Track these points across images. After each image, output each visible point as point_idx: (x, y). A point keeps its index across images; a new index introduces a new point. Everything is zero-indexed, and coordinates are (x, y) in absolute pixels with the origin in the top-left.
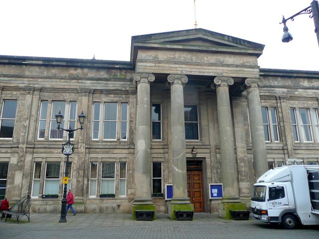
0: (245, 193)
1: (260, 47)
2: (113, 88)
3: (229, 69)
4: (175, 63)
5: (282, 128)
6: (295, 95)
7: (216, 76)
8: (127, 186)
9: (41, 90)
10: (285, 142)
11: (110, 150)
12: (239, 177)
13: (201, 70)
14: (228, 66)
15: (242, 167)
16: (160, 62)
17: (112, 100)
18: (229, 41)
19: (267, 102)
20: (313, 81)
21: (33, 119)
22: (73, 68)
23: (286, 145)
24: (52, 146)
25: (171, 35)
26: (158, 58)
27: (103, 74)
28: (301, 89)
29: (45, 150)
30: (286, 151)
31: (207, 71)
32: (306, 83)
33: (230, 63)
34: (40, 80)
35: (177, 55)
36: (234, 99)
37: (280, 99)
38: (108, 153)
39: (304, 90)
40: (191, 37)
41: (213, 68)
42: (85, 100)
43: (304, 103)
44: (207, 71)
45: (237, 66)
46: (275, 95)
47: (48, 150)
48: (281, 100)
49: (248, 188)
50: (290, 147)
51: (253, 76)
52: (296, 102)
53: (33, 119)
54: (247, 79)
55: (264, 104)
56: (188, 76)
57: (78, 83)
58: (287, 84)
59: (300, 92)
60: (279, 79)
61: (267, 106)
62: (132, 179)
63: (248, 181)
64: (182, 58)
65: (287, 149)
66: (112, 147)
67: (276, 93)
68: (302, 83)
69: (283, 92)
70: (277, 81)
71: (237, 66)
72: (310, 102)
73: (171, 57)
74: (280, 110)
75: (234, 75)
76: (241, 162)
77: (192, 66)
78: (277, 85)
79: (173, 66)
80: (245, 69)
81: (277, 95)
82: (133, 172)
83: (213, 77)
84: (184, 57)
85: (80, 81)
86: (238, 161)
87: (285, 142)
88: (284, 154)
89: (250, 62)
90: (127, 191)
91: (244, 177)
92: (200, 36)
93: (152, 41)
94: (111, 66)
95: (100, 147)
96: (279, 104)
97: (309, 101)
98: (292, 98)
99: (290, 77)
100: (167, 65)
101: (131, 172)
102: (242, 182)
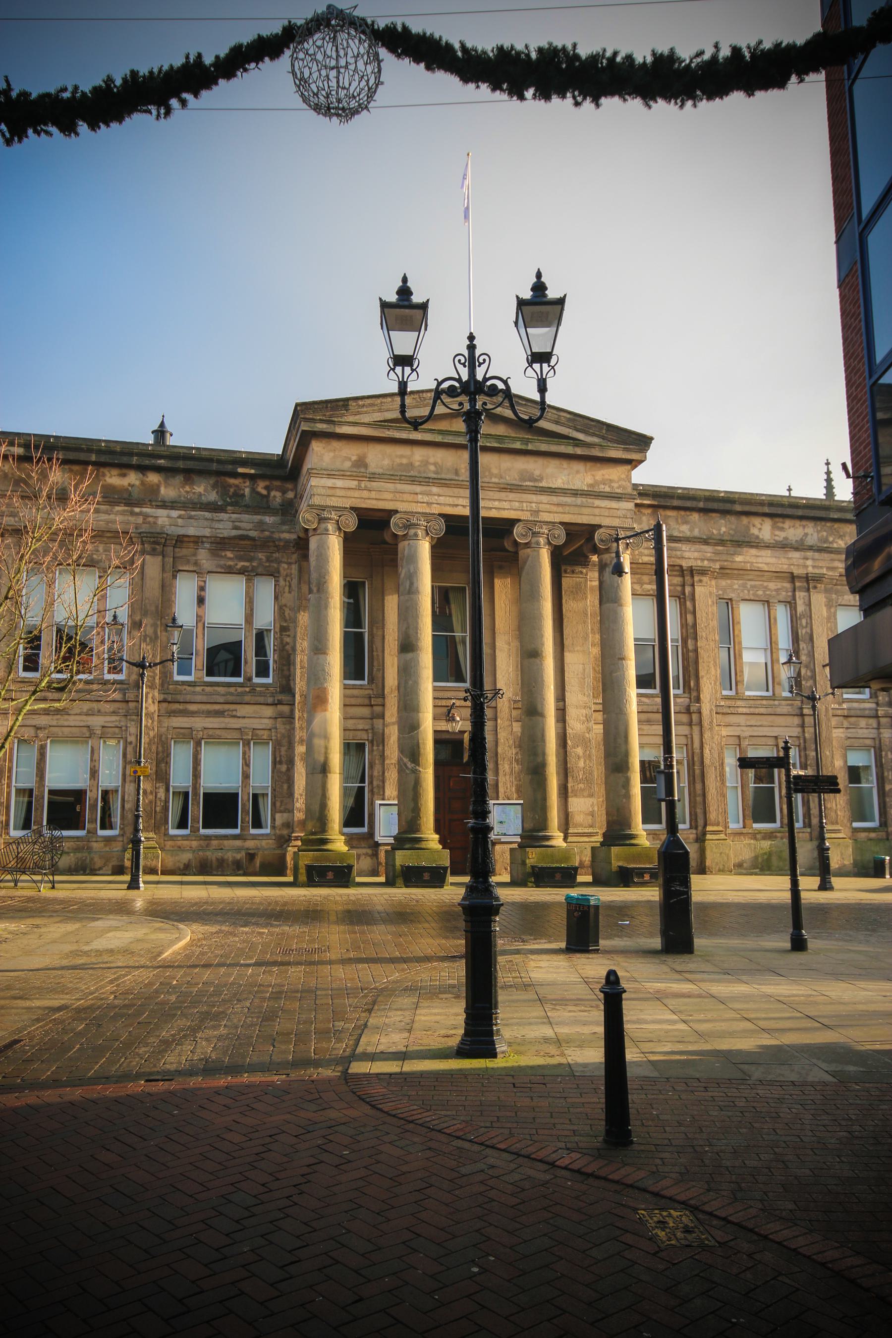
0: (581, 825)
1: (642, 442)
2: (235, 533)
3: (555, 499)
4: (413, 480)
5: (691, 654)
6: (735, 566)
7: (519, 520)
8: (274, 804)
10: (694, 694)
11: (227, 707)
12: (569, 785)
16: (373, 477)
17: (230, 566)
22: (115, 472)
23: (698, 700)
26: (366, 466)
27: (202, 489)
30: (695, 717)
31: (496, 504)
35: (418, 455)
36: (566, 572)
37: (692, 576)
38: (219, 714)
41: (512, 496)
42: (153, 565)
44: (496, 504)
48: (696, 578)
49: (592, 814)
50: (706, 707)
52: (737, 584)
54: (601, 530)
56: (447, 517)
57: (132, 514)
58: (715, 532)
59: (746, 557)
60: (695, 516)
62: (285, 786)
63: (591, 796)
65: (700, 713)
66: (231, 698)
68: (755, 531)
70: (686, 522)
71: (575, 493)
72: (772, 585)
73: (401, 464)
74: (689, 604)
75: (567, 519)
77: (456, 490)
78: (688, 534)
80: (597, 502)
81: (685, 564)
82: (288, 770)
84: (435, 464)
85: (137, 510)
86: (569, 742)
87: (694, 694)
88: (690, 724)
89: (611, 481)
90: (273, 819)
91: (581, 786)
94: (230, 467)
95: (199, 698)
96: (688, 589)
98: (724, 572)
99: (725, 513)
100: (390, 486)
101: (284, 768)
102: (576, 796)
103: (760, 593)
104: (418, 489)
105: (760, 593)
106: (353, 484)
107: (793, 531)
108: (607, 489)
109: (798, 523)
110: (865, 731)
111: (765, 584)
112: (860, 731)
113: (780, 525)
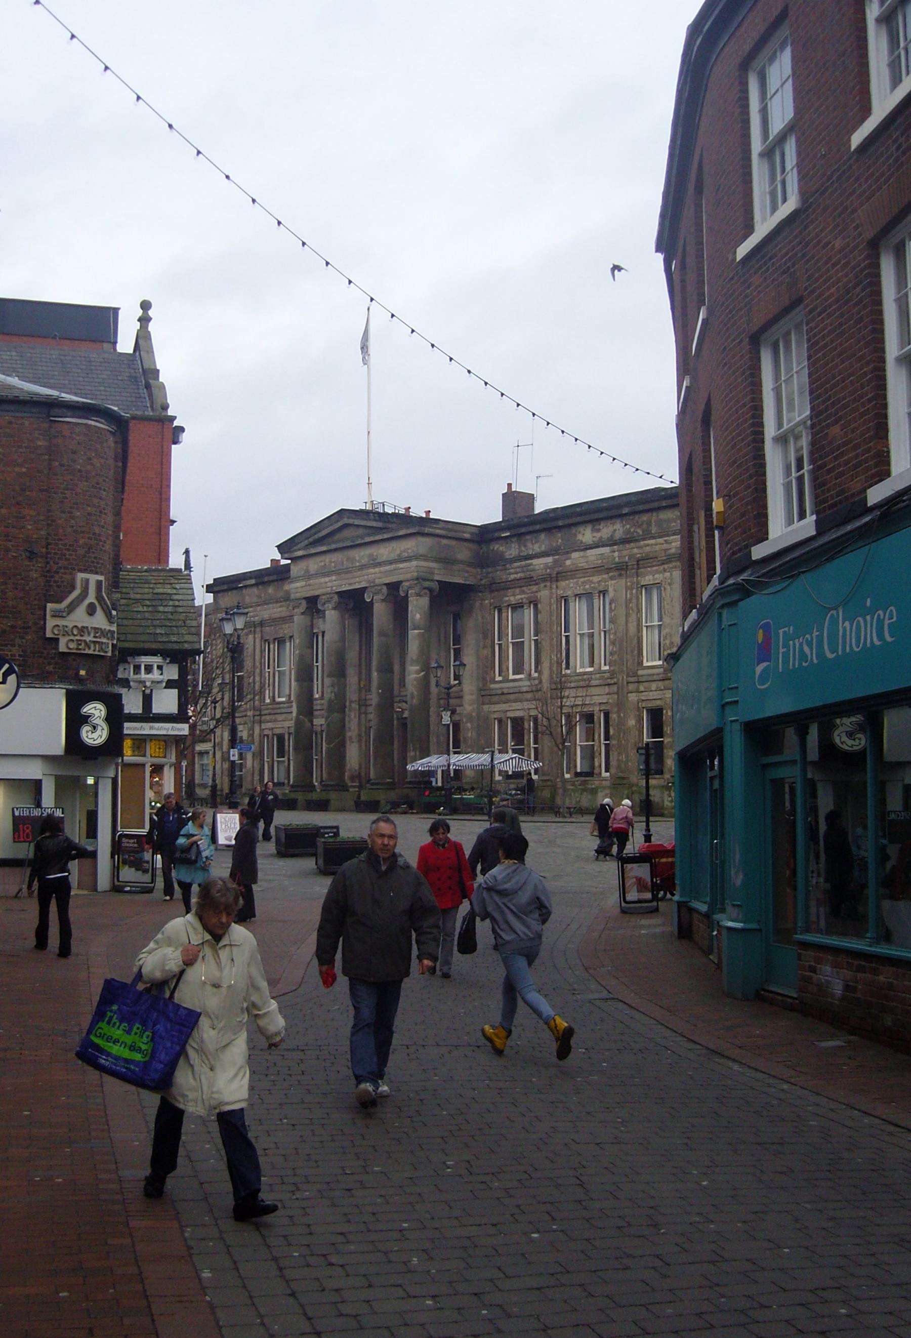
7: (366, 588)
9: (262, 624)
13: (352, 581)
14: (380, 564)
15: (468, 730)
18: (375, 520)
19: (523, 592)
20: (601, 527)
24: (276, 711)
25: (313, 531)
28: (576, 551)
29: (271, 717)
32: (587, 535)
33: (384, 558)
34: (259, 608)
35: (327, 558)
39: (582, 553)
45: (391, 562)
46: (533, 574)
47: (273, 717)
51: (409, 576)
53: (258, 671)
55: (519, 597)
56: (338, 593)
59: (576, 559)
60: (543, 536)
68: (580, 537)
69: (546, 566)
71: (391, 562)
72: (595, 579)
75: (387, 580)
76: (467, 722)
79: (323, 580)
80: (401, 566)
83: (363, 590)
92: (346, 521)
93: (299, 546)
97: (593, 575)
103: (587, 587)
104: (327, 579)
105: (587, 587)
106: (303, 583)
107: (607, 530)
108: (406, 555)
109: (610, 522)
110: (655, 693)
112: (651, 693)
113: (597, 527)
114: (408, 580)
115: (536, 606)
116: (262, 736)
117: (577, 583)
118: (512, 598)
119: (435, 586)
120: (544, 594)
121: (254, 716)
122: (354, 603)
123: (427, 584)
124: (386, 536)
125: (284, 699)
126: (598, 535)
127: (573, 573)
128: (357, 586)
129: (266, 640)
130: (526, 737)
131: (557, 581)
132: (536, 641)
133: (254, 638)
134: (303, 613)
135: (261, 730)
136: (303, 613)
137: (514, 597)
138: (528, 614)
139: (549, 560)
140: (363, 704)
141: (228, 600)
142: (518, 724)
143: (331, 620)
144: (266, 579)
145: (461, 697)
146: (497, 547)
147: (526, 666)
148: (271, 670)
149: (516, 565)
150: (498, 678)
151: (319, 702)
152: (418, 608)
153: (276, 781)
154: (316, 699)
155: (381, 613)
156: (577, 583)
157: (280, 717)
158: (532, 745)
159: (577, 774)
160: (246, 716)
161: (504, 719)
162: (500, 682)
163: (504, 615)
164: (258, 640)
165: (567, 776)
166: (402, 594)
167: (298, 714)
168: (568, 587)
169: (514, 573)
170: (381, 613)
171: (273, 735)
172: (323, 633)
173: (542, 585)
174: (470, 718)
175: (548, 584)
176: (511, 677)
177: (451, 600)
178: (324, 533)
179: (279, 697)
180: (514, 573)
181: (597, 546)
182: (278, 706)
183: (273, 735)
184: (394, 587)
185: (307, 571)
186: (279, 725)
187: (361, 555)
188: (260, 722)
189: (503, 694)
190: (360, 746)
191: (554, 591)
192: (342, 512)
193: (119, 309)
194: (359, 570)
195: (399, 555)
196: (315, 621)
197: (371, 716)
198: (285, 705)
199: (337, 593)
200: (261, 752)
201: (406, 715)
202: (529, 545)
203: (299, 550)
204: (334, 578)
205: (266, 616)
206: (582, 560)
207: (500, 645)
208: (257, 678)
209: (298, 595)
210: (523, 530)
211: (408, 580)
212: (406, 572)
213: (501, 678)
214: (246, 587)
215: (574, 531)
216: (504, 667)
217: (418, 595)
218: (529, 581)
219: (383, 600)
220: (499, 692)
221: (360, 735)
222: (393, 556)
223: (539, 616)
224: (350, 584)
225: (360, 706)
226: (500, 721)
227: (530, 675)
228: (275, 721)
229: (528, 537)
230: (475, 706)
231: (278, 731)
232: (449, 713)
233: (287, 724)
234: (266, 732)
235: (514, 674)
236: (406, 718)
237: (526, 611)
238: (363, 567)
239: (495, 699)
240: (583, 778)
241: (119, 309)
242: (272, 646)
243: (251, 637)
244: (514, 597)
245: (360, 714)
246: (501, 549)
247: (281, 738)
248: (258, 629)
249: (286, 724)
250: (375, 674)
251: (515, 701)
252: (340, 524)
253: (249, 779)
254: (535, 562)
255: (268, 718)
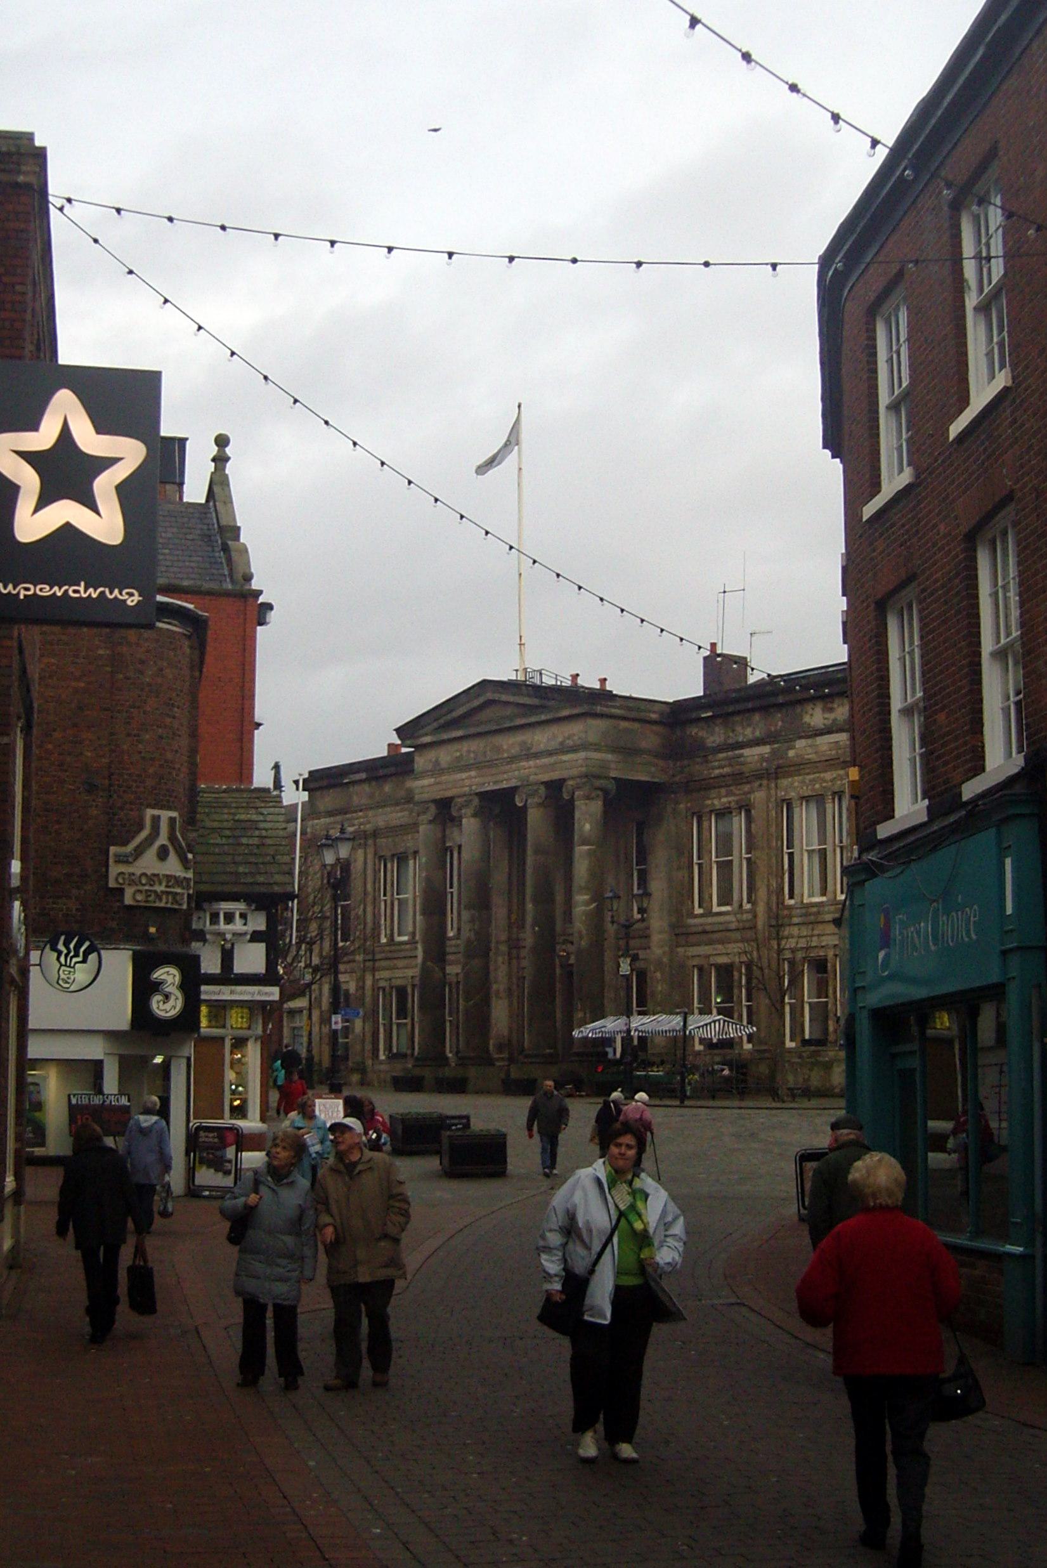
9: (375, 834)
13: (500, 777)
14: (537, 755)
18: (529, 696)
21: (370, 898)
24: (396, 955)
25: (445, 710)
28: (801, 738)
34: (370, 813)
35: (465, 746)
39: (810, 741)
40: (476, 703)
43: (813, 780)
45: (550, 754)
51: (575, 772)
53: (370, 898)
55: (724, 800)
56: (482, 795)
60: (757, 717)
61: (733, 805)
64: (472, 755)
67: (743, 764)
68: (807, 719)
69: (762, 758)
72: (828, 776)
75: (546, 777)
79: (459, 776)
80: (565, 758)
83: (513, 791)
92: (489, 696)
97: (826, 771)
104: (464, 775)
105: (817, 786)
111: (822, 775)
113: (830, 705)
114: (573, 778)
115: (748, 812)
116: (376, 989)
117: (803, 782)
118: (716, 802)
119: (611, 786)
120: (758, 796)
121: (365, 961)
122: (500, 808)
123: (598, 783)
124: (543, 717)
125: (405, 938)
126: (832, 716)
127: (799, 767)
128: (505, 785)
129: (380, 857)
130: (736, 991)
131: (777, 778)
132: (749, 860)
133: (365, 854)
134: (430, 822)
135: (375, 981)
136: (430, 822)
137: (719, 801)
138: (738, 823)
139: (766, 749)
140: (514, 945)
141: (329, 800)
142: (726, 972)
143: (469, 832)
144: (381, 772)
145: (647, 937)
146: (693, 730)
147: (736, 896)
148: (388, 898)
149: (721, 756)
150: (698, 911)
151: (454, 942)
152: (587, 817)
153: (395, 1051)
154: (450, 939)
155: (536, 819)
156: (803, 782)
157: (400, 963)
158: (744, 1003)
159: (805, 1043)
160: (354, 961)
161: (706, 966)
162: (702, 916)
163: (705, 824)
164: (370, 856)
165: (790, 1044)
166: (566, 796)
167: (424, 962)
168: (793, 786)
169: (718, 767)
170: (536, 819)
171: (392, 988)
172: (460, 847)
173: (757, 784)
174: (659, 964)
175: (765, 782)
176: (716, 909)
177: (634, 807)
178: (461, 711)
179: (399, 935)
180: (718, 767)
181: (830, 732)
182: (398, 948)
183: (392, 988)
184: (555, 787)
185: (437, 763)
186: (398, 973)
187: (510, 743)
188: (374, 970)
189: (705, 932)
190: (511, 1004)
191: (773, 792)
192: (484, 683)
193: (187, 439)
194: (508, 763)
195: (562, 743)
196: (448, 832)
197: (525, 963)
198: (408, 947)
199: (477, 794)
200: (375, 1012)
201: (572, 961)
202: (739, 729)
203: (426, 734)
204: (473, 773)
205: (381, 824)
206: (809, 750)
207: (700, 865)
208: (369, 909)
209: (426, 796)
210: (731, 709)
211: (573, 778)
212: (572, 765)
213: (701, 911)
214: (353, 783)
215: (798, 710)
216: (707, 897)
217: (588, 798)
218: (739, 778)
219: (539, 805)
220: (700, 929)
221: (510, 989)
222: (554, 745)
223: (753, 825)
224: (495, 783)
225: (510, 948)
226: (701, 969)
227: (741, 906)
228: (395, 968)
229: (737, 718)
230: (667, 949)
231: (399, 982)
232: (628, 960)
233: (410, 973)
234: (382, 984)
235: (719, 905)
236: (572, 965)
237: (735, 820)
238: (513, 759)
239: (692, 939)
240: (813, 1048)
241: (187, 439)
242: (389, 865)
243: (360, 852)
244: (719, 801)
245: (510, 959)
246: (700, 734)
247: (402, 992)
248: (370, 842)
249: (408, 972)
250: (529, 906)
251: (722, 942)
252: (481, 700)
253: (358, 1047)
254: (746, 752)
255: (383, 963)
